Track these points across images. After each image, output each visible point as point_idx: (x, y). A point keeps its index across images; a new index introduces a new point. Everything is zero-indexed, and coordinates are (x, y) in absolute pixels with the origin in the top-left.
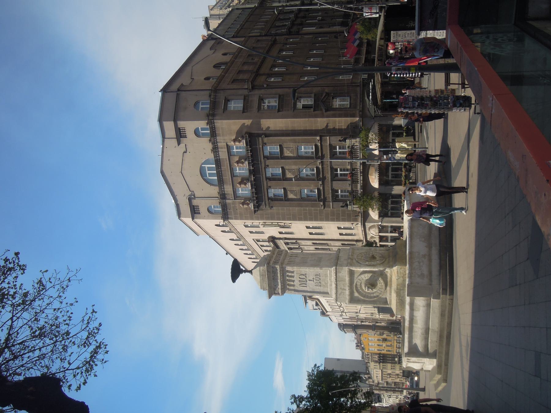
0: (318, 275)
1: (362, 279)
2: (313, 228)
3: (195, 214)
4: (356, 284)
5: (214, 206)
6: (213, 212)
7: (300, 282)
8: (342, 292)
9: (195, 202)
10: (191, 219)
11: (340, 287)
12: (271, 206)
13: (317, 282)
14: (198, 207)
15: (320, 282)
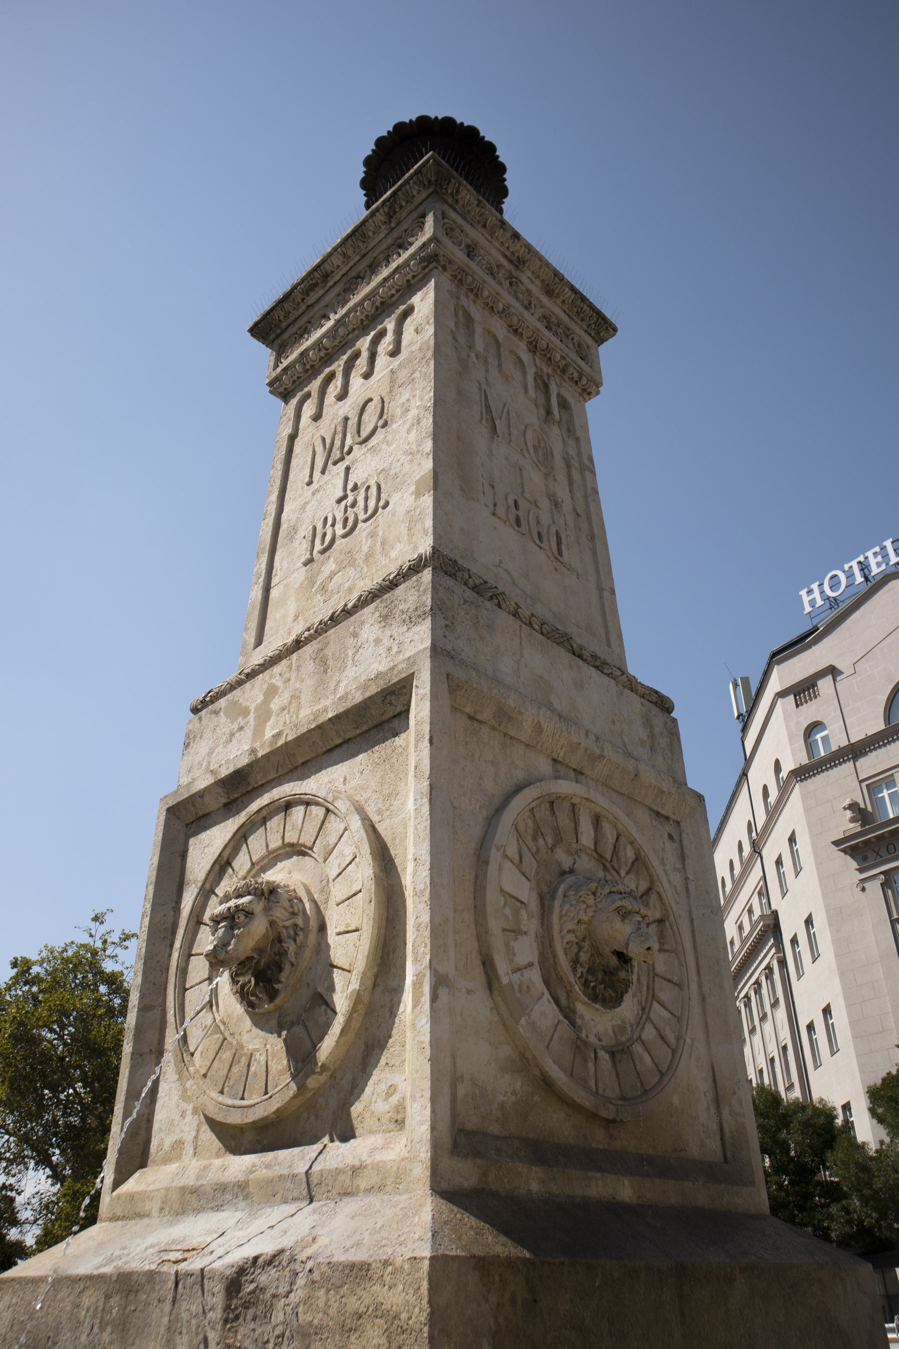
0: (378, 499)
1: (333, 840)
2: (830, 1030)
3: (795, 696)
4: (287, 806)
5: (827, 735)
6: (811, 739)
7: (340, 428)
8: (245, 712)
9: (825, 685)
10: (780, 690)
11: (278, 682)
12: (866, 885)
13: (333, 525)
14: (816, 697)
15: (333, 541)
